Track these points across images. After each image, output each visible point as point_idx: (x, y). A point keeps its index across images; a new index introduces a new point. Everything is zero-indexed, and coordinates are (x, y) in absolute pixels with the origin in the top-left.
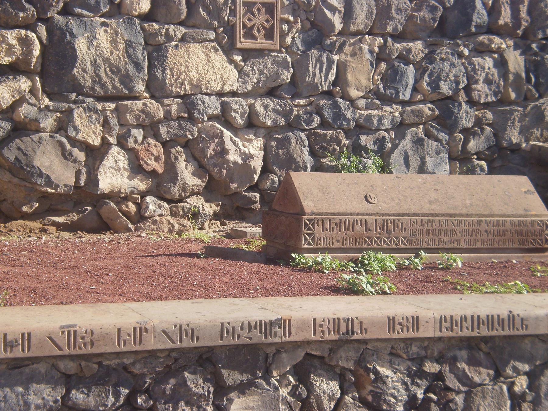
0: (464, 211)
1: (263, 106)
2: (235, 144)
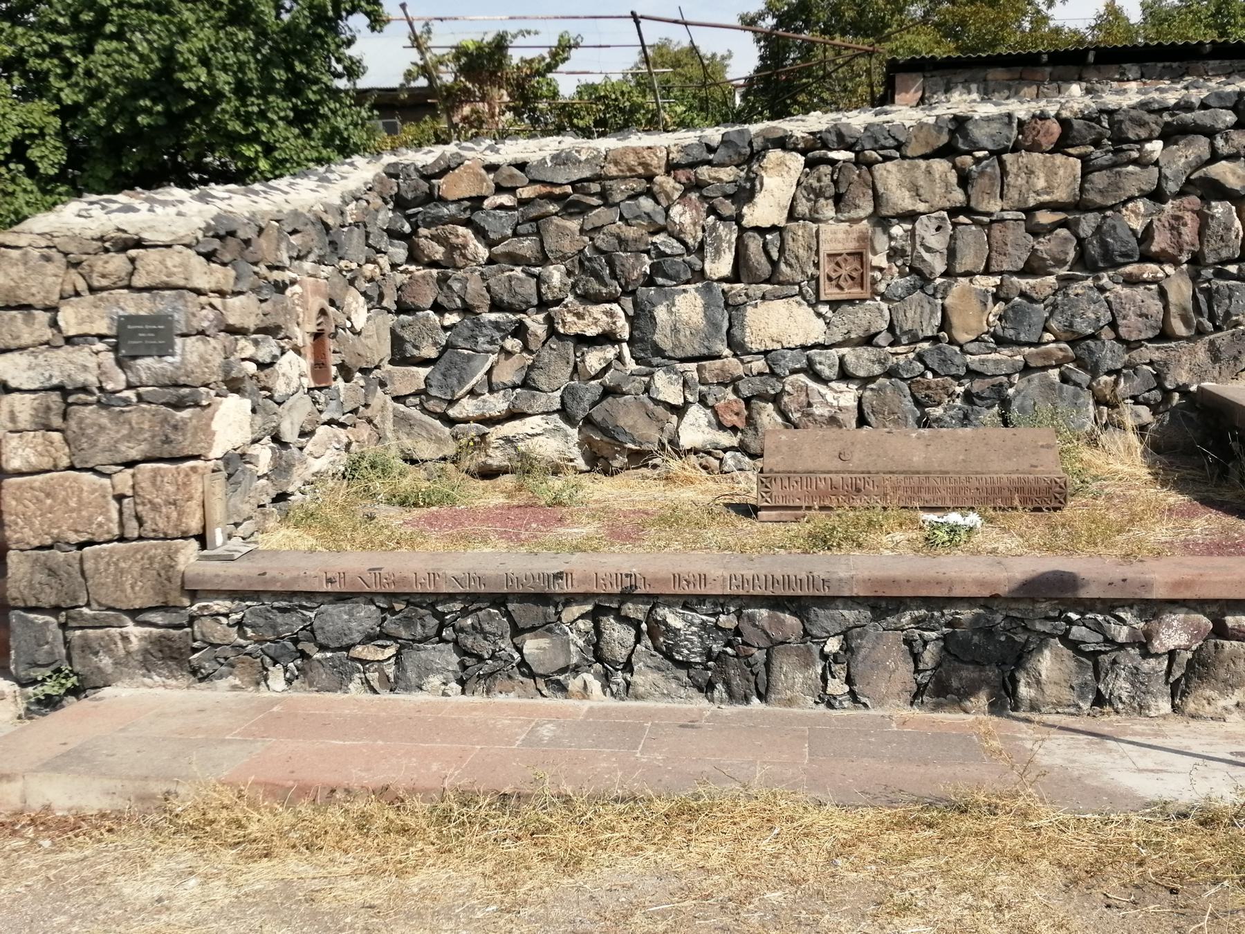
2: (823, 396)
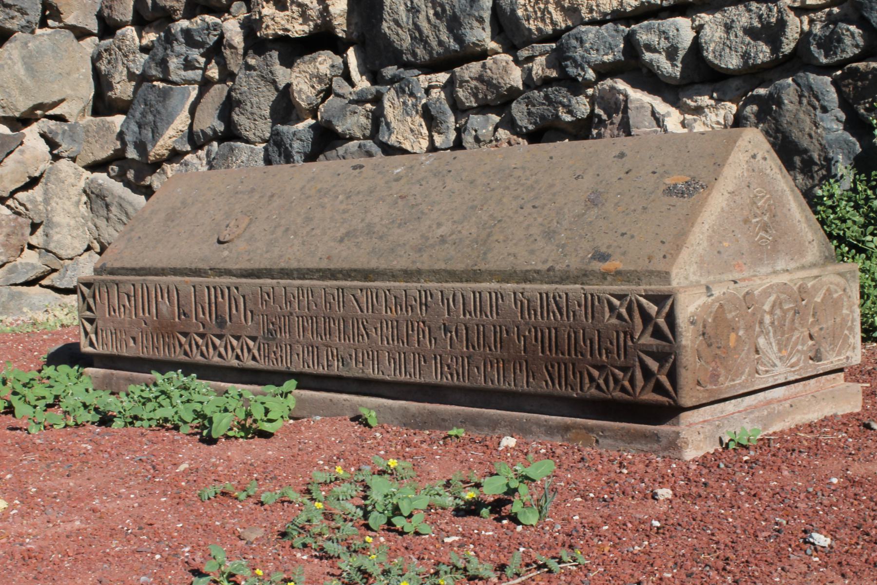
0: (400, 263)
1: (726, 25)
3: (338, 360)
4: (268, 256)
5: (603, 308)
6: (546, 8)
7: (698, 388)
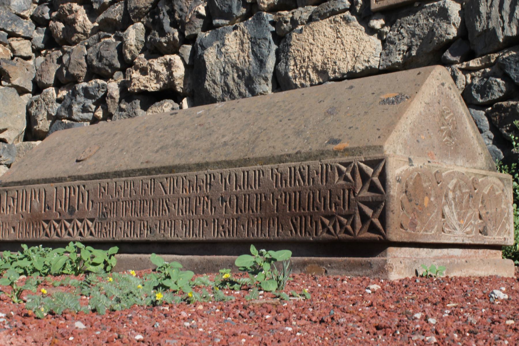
3: (147, 230)
4: (108, 165)
5: (334, 174)
6: (307, 71)
7: (402, 230)
